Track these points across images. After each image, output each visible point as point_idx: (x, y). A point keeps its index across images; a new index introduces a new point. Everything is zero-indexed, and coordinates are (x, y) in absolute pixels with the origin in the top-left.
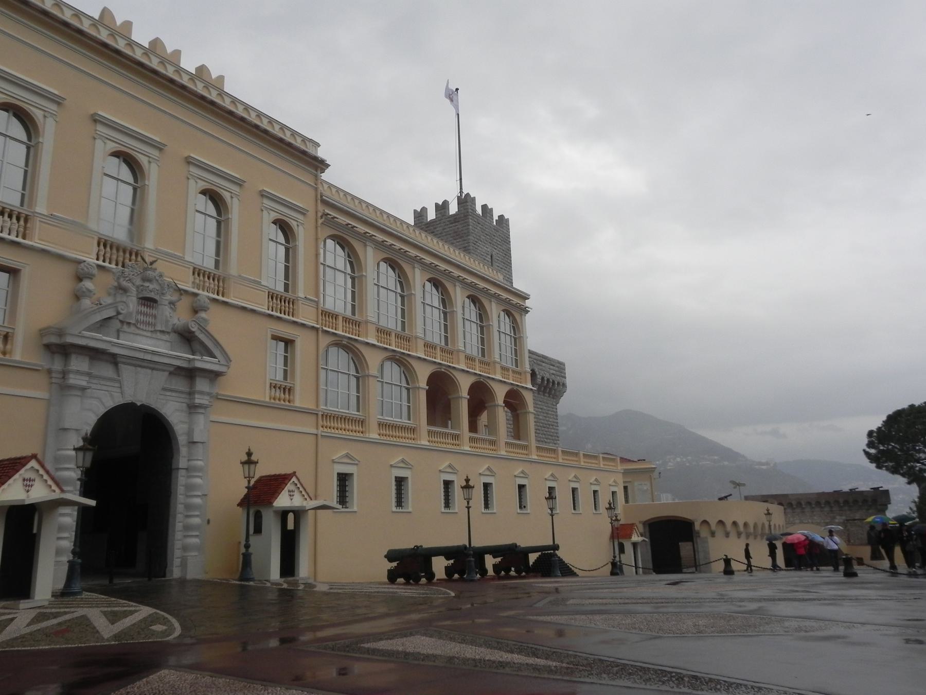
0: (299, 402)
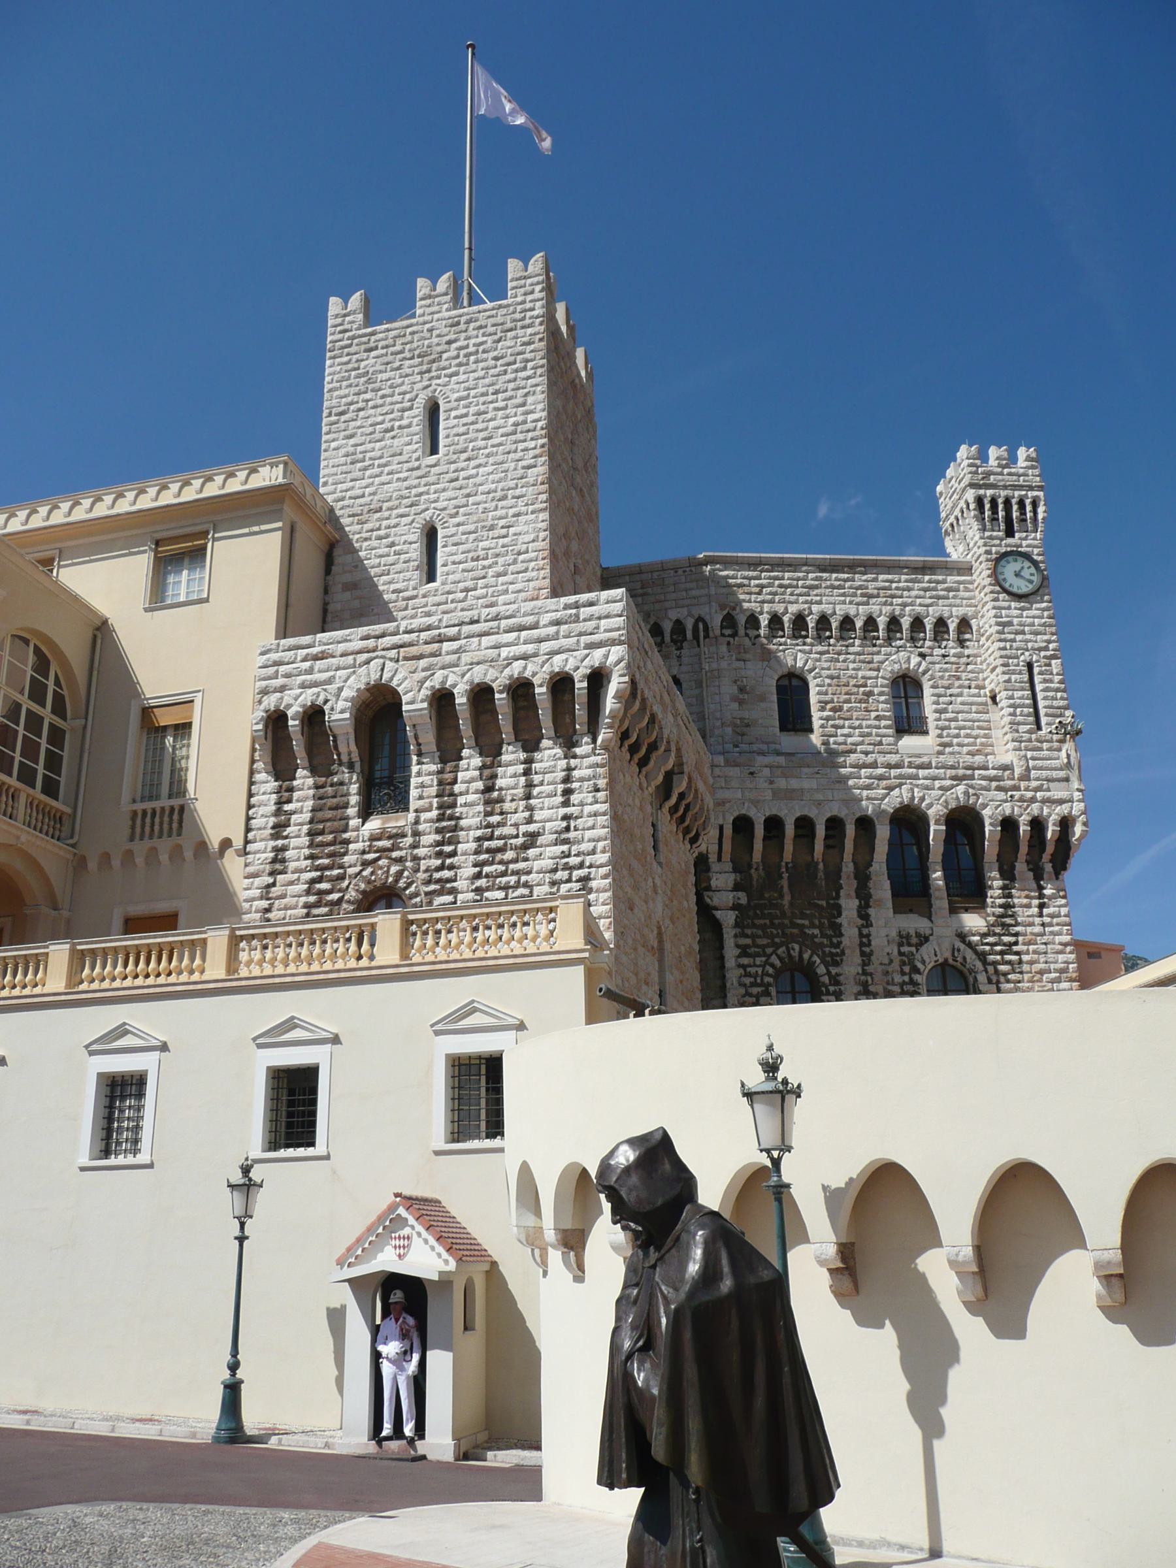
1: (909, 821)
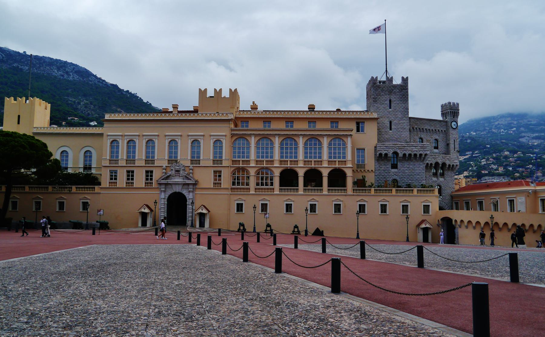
1: (437, 164)
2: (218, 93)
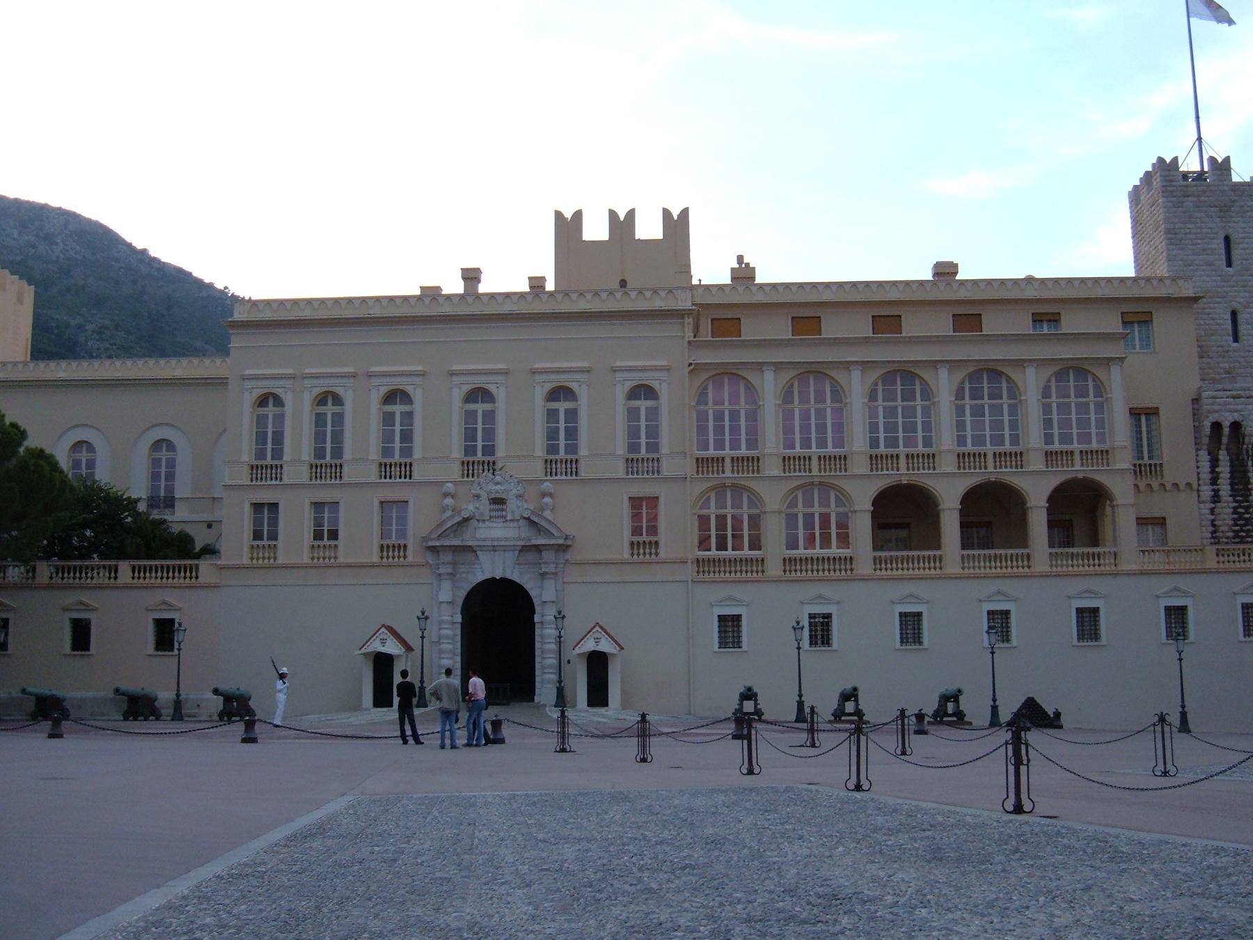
0: (663, 554)
2: (622, 225)
